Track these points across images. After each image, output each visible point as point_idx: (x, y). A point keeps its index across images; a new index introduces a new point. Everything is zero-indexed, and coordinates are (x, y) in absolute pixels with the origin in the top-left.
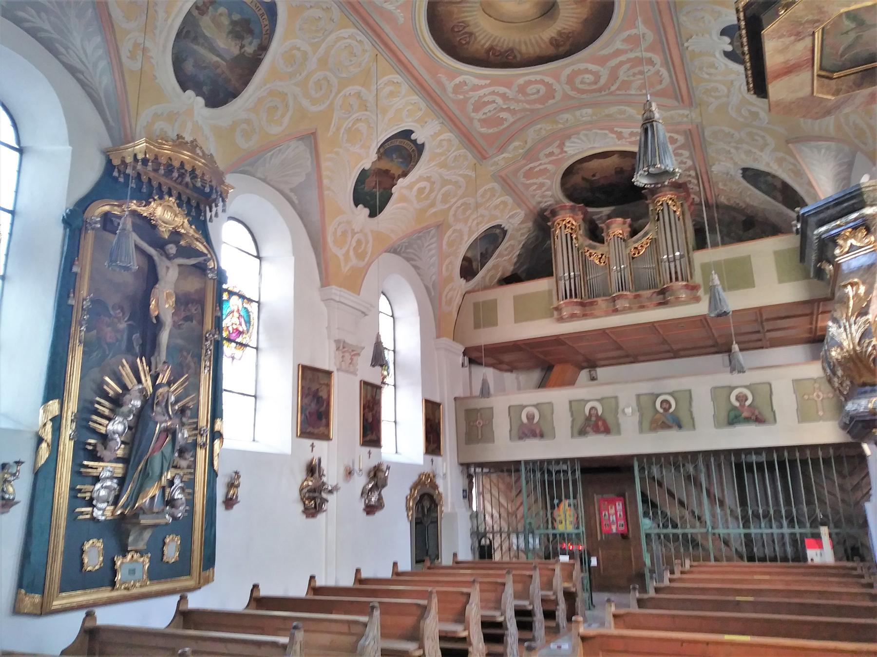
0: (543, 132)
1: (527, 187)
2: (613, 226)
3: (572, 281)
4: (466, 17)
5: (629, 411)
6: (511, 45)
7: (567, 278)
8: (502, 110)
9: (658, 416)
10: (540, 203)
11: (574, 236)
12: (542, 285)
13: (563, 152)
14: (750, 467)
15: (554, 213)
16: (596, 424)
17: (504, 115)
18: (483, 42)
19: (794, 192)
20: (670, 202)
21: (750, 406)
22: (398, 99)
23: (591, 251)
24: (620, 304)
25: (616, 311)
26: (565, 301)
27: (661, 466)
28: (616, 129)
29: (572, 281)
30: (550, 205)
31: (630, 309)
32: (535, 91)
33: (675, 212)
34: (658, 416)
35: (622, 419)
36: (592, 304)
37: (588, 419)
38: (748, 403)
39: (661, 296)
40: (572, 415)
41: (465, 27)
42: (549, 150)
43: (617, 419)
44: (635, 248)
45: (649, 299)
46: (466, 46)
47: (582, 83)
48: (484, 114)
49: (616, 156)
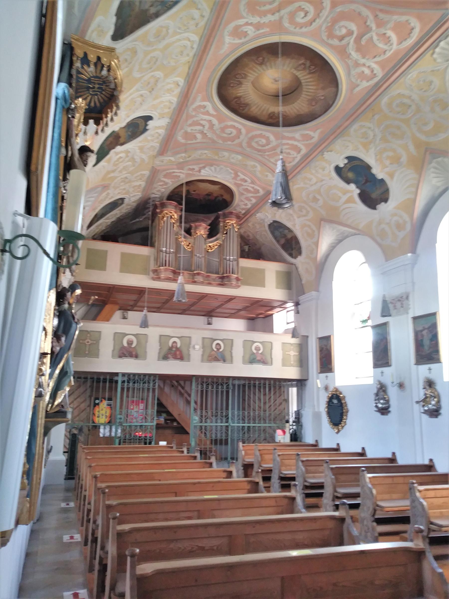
0: (204, 157)
4: (251, 74)
5: (197, 347)
6: (250, 102)
8: (202, 132)
9: (213, 353)
12: (144, 251)
13: (200, 171)
14: (234, 385)
15: (163, 205)
16: (174, 353)
17: (199, 136)
18: (240, 91)
19: (297, 242)
21: (261, 353)
22: (169, 95)
25: (194, 282)
27: (198, 384)
28: (239, 174)
31: (202, 283)
32: (230, 132)
34: (213, 353)
35: (192, 352)
37: (170, 349)
38: (260, 352)
39: (220, 280)
40: (160, 345)
41: (242, 78)
43: (189, 351)
44: (210, 246)
46: (230, 88)
47: (257, 142)
48: (192, 130)
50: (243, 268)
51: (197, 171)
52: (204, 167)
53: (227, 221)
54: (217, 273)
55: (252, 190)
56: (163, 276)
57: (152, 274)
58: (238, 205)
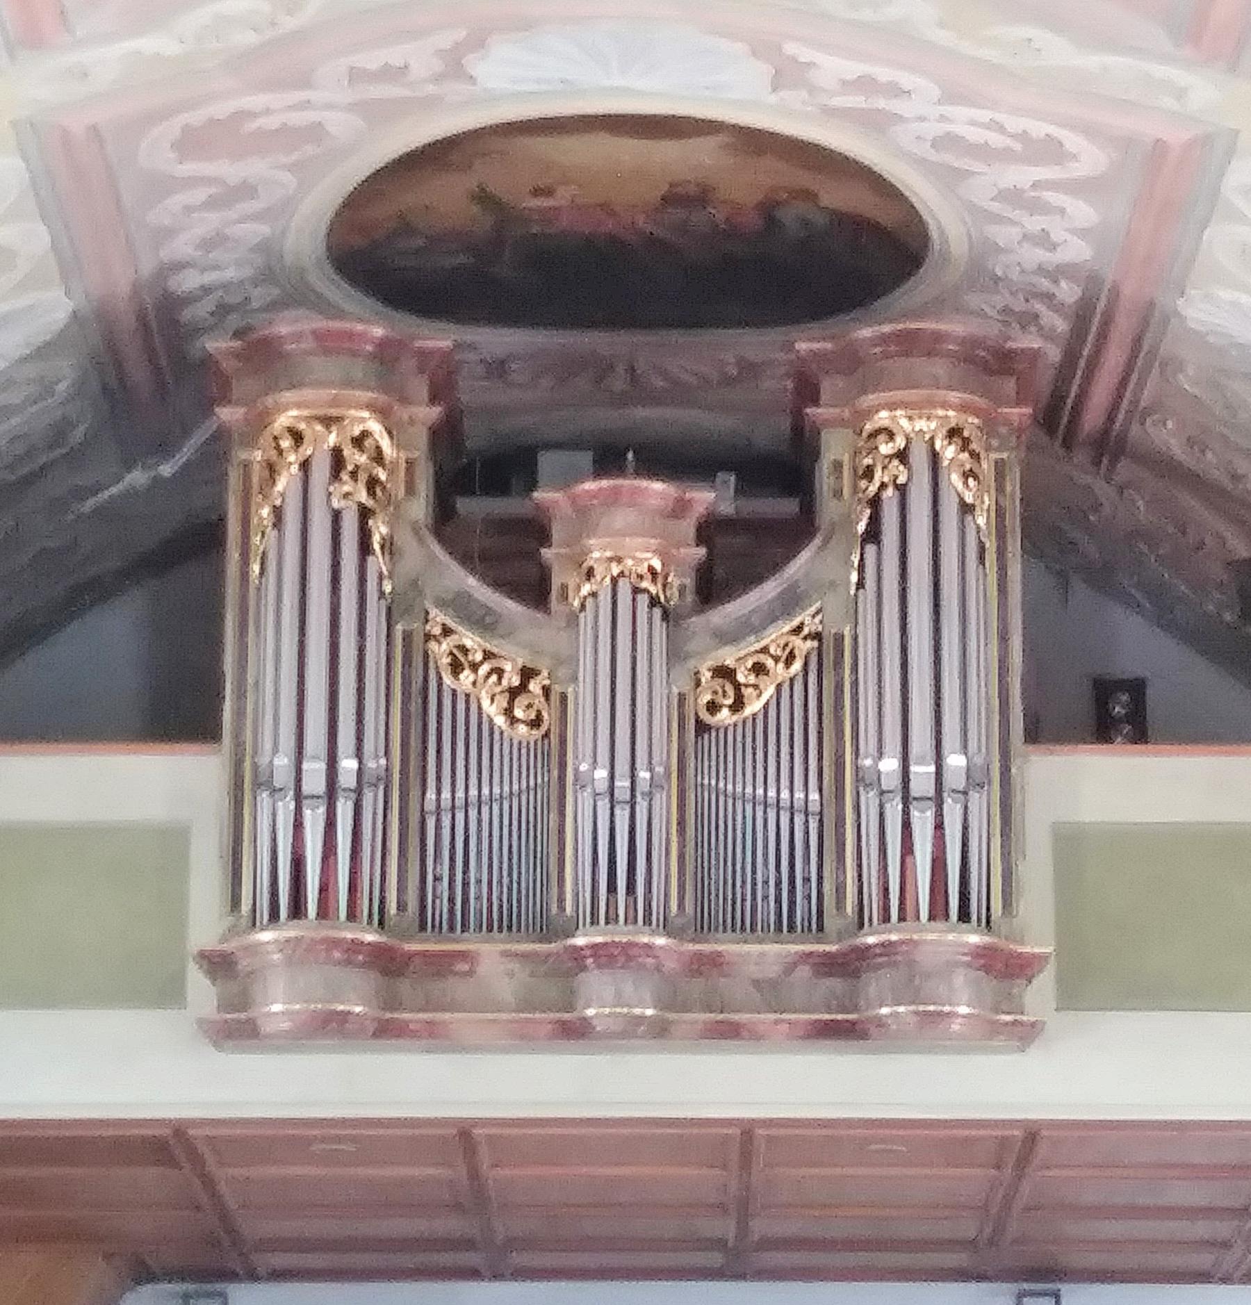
1: (165, 185)
2: (621, 518)
3: (344, 810)
7: (315, 780)
10: (179, 266)
11: (380, 530)
13: (454, 66)
15: (264, 357)
20: (950, 452)
23: (470, 640)
24: (601, 997)
25: (575, 1032)
26: (290, 931)
28: (790, 48)
29: (344, 810)
30: (225, 286)
33: (966, 509)
36: (441, 965)
39: (836, 984)
42: (394, 55)
44: (723, 673)
45: (771, 993)
49: (721, 138)
50: (1070, 842)
51: (438, 79)
52: (477, 42)
53: (883, 418)
54: (785, 926)
55: (996, 140)
56: (277, 1006)
57: (202, 992)
58: (982, 252)
